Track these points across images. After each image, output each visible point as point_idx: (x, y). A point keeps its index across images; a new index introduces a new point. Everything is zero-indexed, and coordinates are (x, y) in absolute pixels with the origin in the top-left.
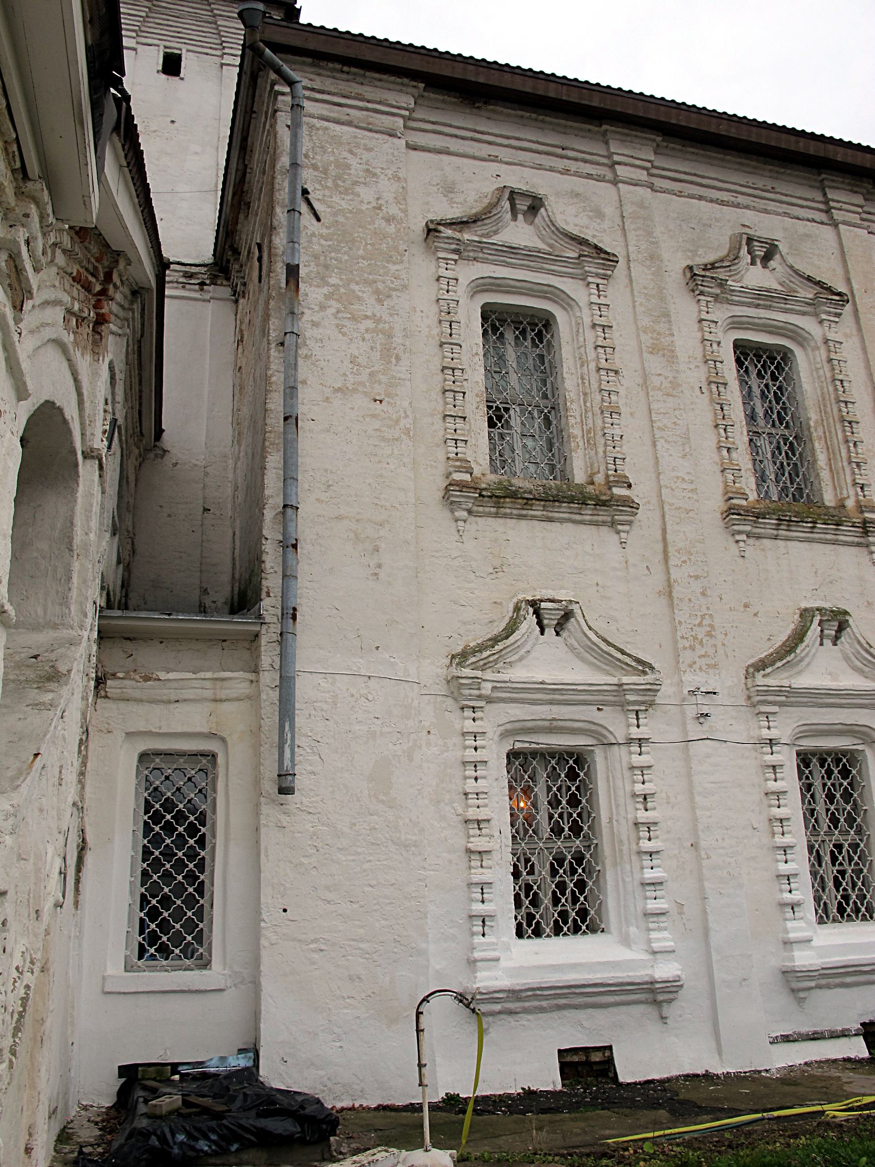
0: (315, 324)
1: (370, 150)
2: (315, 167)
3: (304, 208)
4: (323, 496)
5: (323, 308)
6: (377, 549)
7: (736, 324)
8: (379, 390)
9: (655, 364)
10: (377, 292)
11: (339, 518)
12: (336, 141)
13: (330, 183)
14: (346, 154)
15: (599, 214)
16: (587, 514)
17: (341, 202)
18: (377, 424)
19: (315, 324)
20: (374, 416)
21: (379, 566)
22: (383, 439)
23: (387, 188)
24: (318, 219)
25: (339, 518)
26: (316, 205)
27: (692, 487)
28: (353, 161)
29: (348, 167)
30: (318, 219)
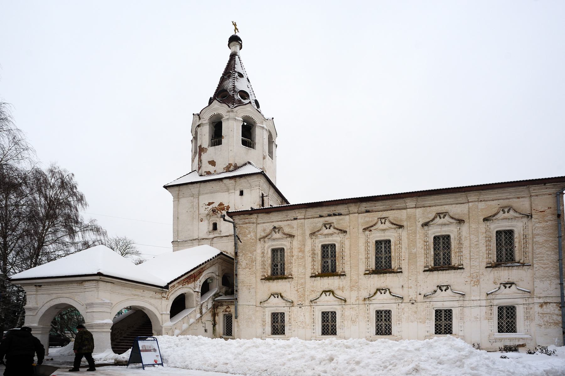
0: (241, 259)
1: (250, 228)
2: (240, 234)
3: (239, 241)
4: (242, 283)
5: (242, 256)
6: (250, 289)
7: (321, 242)
8: (250, 267)
9: (300, 254)
10: (251, 252)
11: (244, 286)
12: (244, 228)
13: (243, 236)
14: (246, 230)
15: (293, 228)
16: (284, 280)
17: (245, 238)
18: (250, 272)
19: (241, 259)
20: (250, 271)
21: (250, 291)
22: (251, 274)
23: (252, 234)
24: (241, 242)
25: (244, 286)
26: (241, 240)
27: (304, 274)
28: (247, 231)
29: (246, 232)
30: (241, 242)
